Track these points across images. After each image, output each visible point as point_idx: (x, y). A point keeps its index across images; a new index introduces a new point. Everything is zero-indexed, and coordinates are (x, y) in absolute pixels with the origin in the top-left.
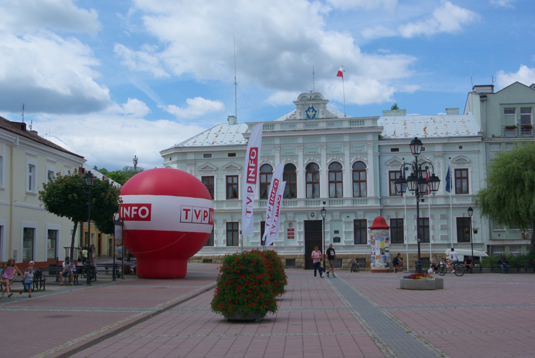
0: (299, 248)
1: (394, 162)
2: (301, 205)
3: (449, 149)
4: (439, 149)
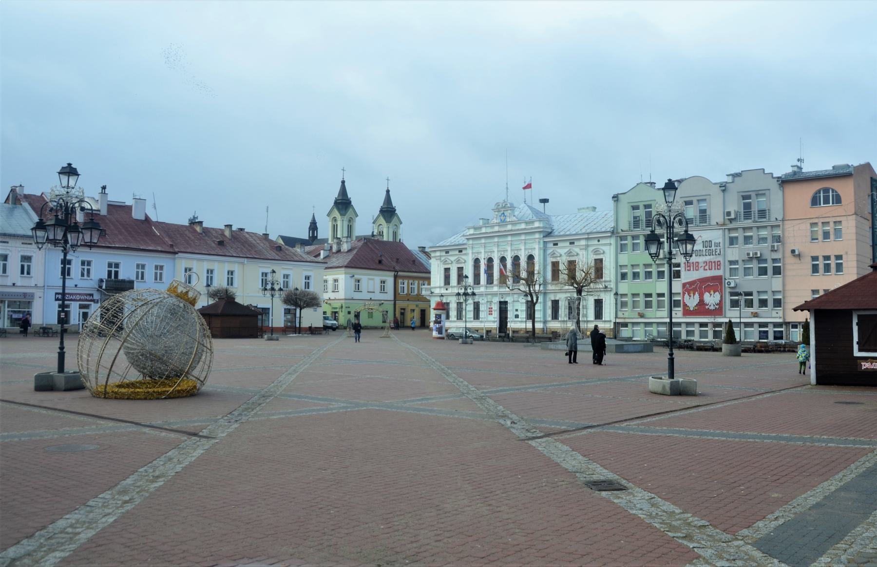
0: (494, 322)
2: (496, 289)
3: (590, 243)
4: (583, 243)
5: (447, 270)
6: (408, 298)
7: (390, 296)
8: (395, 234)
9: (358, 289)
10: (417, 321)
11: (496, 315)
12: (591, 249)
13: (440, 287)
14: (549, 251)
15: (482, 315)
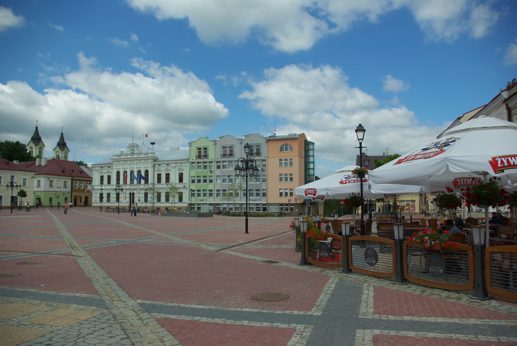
1: (158, 170)
4: (173, 165)
5: (102, 177)
6: (79, 190)
7: (69, 189)
8: (66, 157)
9: (51, 185)
10: (82, 204)
11: (128, 199)
12: (177, 168)
13: (98, 185)
14: (156, 169)
15: (120, 199)
